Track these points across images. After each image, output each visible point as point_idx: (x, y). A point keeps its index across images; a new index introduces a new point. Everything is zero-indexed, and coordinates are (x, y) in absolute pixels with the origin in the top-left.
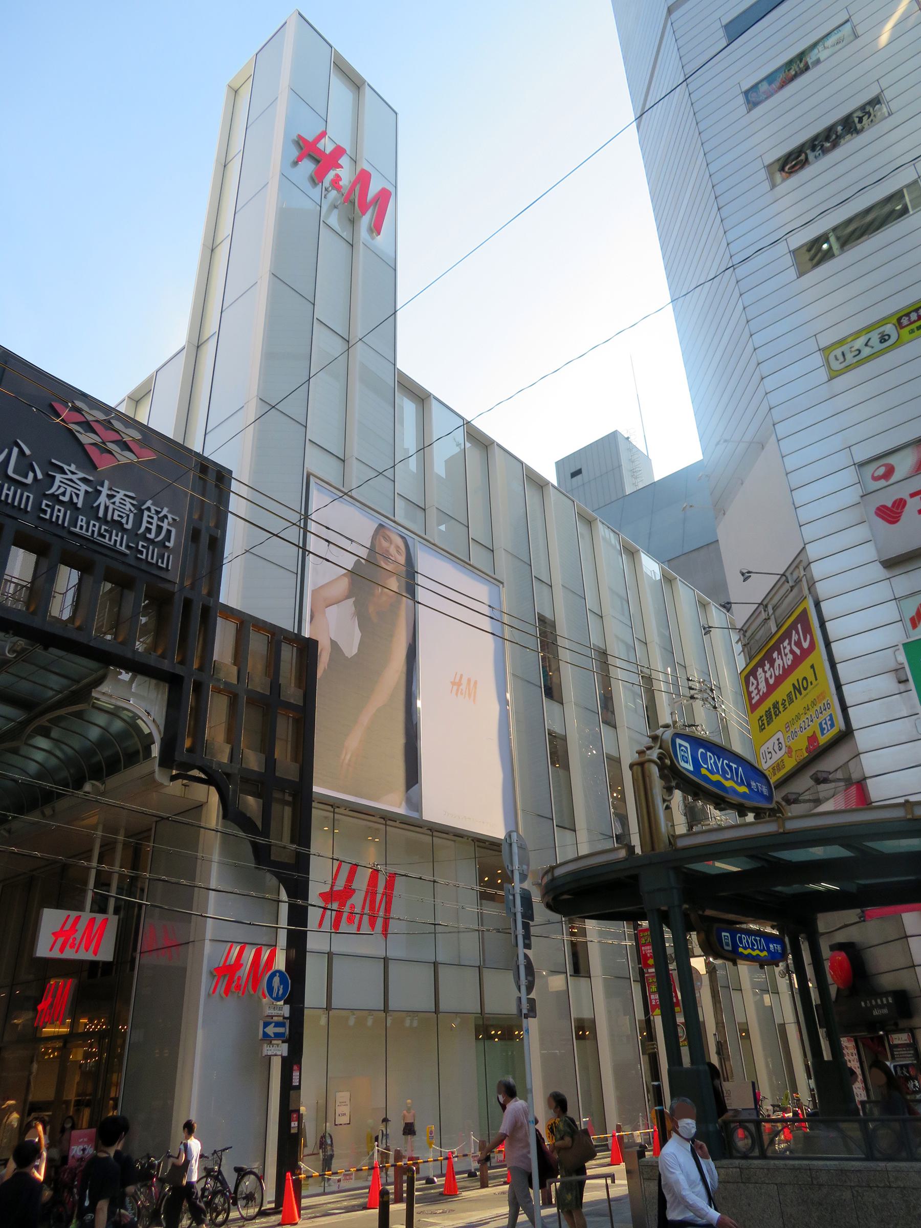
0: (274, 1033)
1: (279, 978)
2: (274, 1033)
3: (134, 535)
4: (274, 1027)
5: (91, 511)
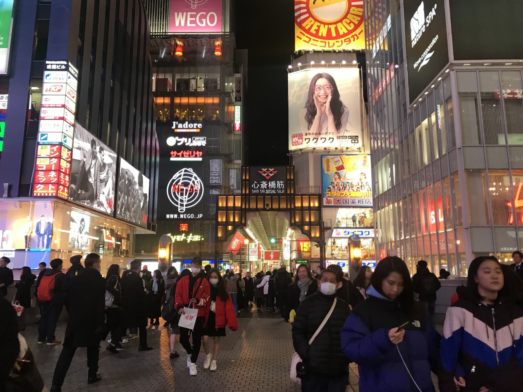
3: (276, 189)
5: (268, 188)
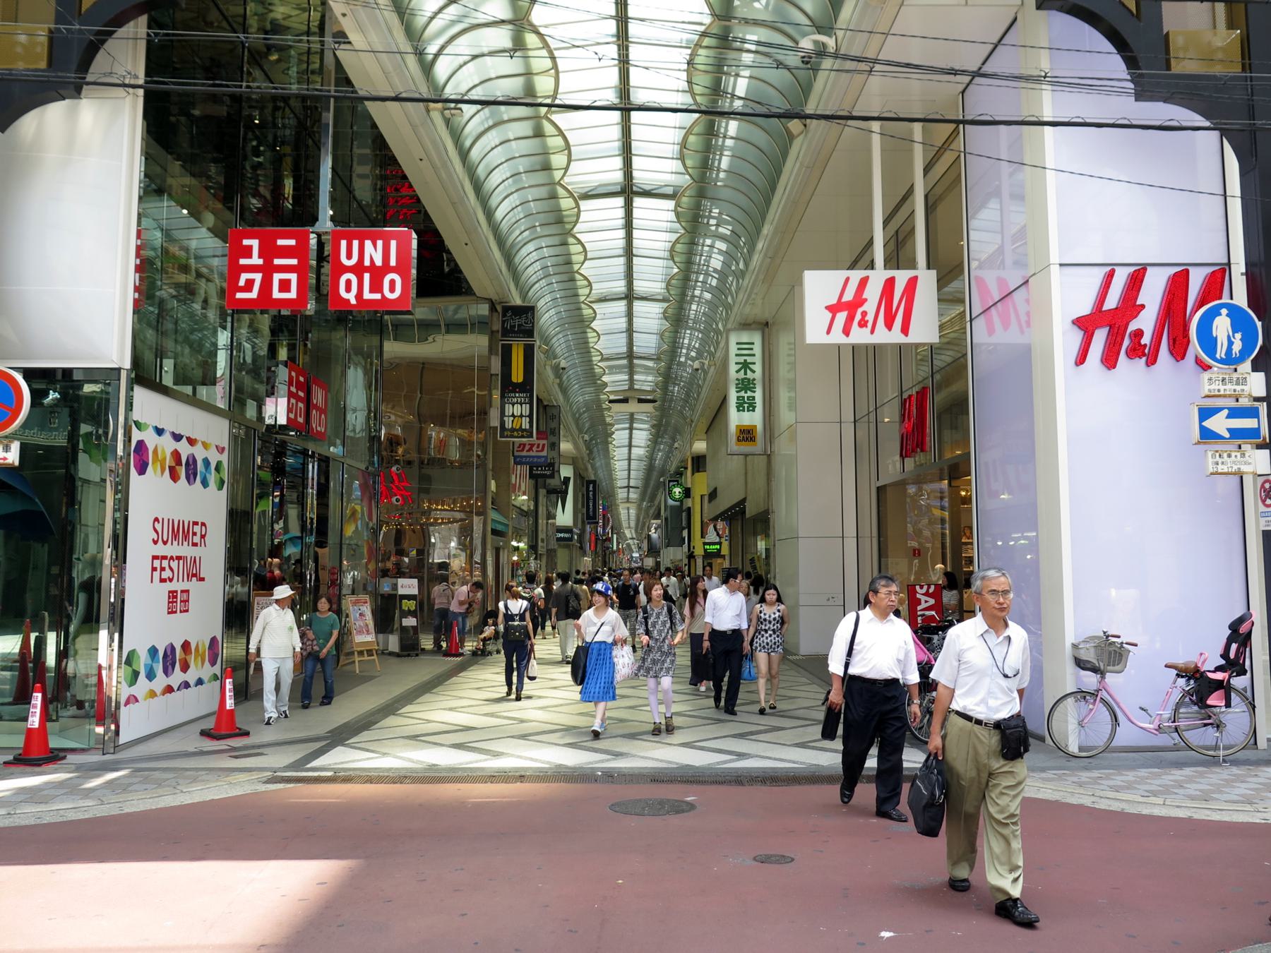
0: (1229, 430)
1: (1228, 320)
2: (1229, 430)
4: (1228, 417)
